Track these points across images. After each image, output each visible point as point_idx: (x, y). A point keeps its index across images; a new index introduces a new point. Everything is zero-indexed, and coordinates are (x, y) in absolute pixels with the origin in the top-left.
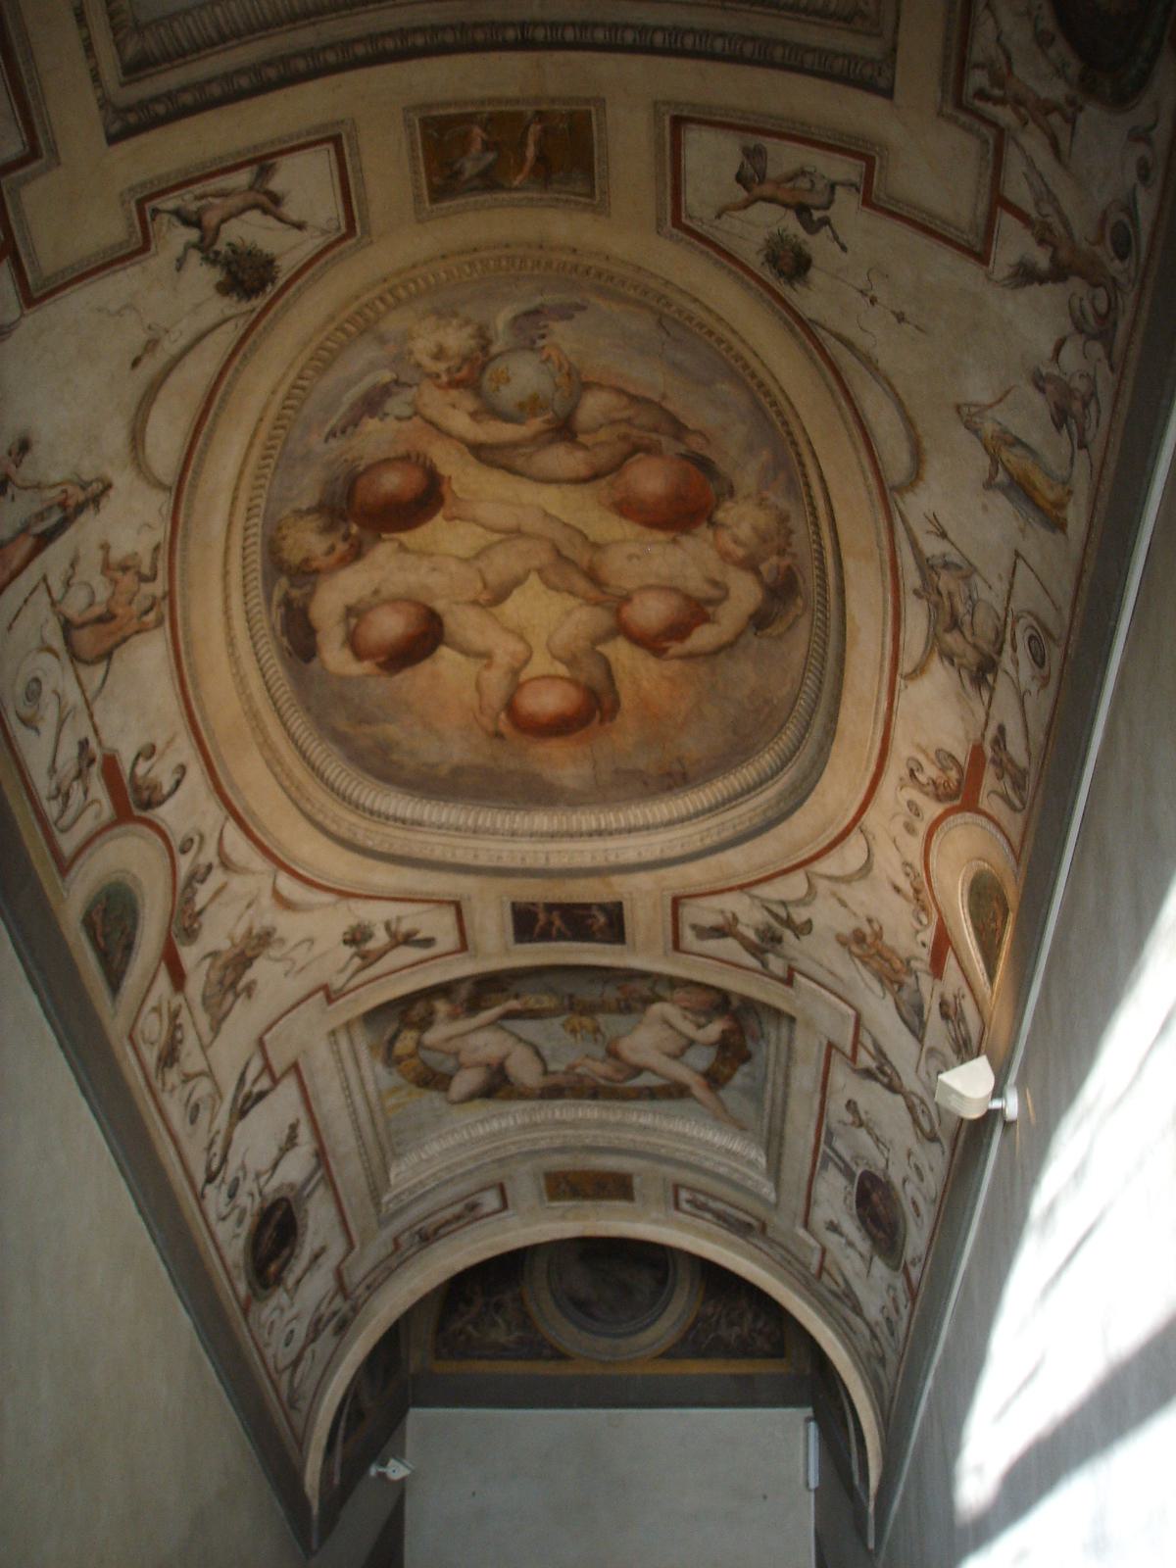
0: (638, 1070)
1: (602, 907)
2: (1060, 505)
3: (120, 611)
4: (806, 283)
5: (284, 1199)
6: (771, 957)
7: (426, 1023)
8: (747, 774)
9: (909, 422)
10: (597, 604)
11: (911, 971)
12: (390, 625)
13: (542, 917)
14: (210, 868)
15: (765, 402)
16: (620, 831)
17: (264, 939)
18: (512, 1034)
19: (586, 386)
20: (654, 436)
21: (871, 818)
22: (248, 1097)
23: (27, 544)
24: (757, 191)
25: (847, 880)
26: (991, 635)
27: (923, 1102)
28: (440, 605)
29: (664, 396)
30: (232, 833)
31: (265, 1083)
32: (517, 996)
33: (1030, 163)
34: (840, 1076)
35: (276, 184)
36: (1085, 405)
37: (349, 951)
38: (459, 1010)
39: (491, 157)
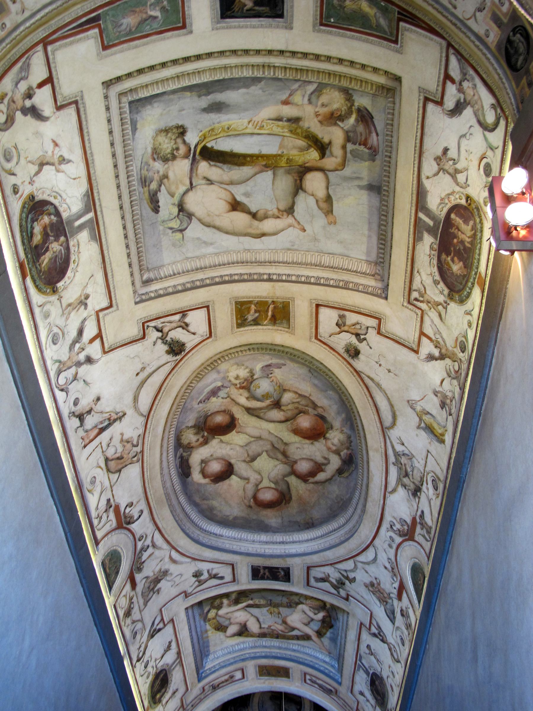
0: (293, 629)
1: (283, 569)
2: (443, 435)
3: (125, 456)
4: (358, 359)
5: (165, 670)
6: (341, 590)
7: (219, 607)
8: (334, 525)
9: (392, 406)
10: (286, 463)
11: (390, 598)
12: (215, 467)
13: (262, 571)
14: (148, 546)
15: (344, 398)
16: (290, 542)
17: (165, 573)
18: (249, 612)
19: (285, 390)
20: (307, 408)
21: (377, 542)
22: (155, 630)
23: (96, 431)
24: (343, 329)
25: (368, 563)
26: (419, 479)
27: (394, 647)
28: (233, 461)
29: (310, 395)
30: (157, 535)
31: (161, 625)
32: (252, 599)
33: (432, 321)
34: (365, 635)
35: (187, 320)
36: (451, 401)
37: (194, 579)
39: (257, 315)
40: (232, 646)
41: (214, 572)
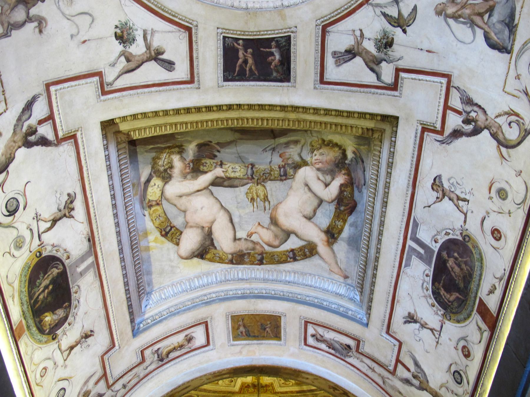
0: (288, 234)
7: (166, 176)
13: (241, 54)
32: (221, 164)
37: (119, 48)
38: (188, 171)
40: (189, 280)
41: (156, 43)
